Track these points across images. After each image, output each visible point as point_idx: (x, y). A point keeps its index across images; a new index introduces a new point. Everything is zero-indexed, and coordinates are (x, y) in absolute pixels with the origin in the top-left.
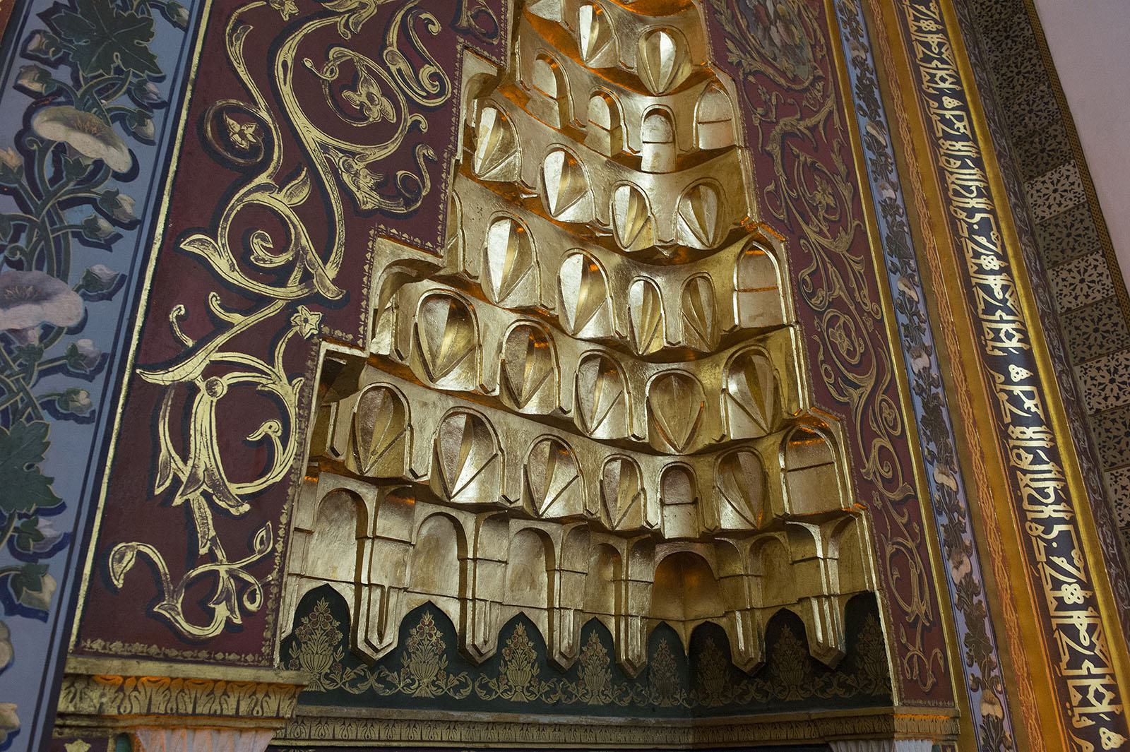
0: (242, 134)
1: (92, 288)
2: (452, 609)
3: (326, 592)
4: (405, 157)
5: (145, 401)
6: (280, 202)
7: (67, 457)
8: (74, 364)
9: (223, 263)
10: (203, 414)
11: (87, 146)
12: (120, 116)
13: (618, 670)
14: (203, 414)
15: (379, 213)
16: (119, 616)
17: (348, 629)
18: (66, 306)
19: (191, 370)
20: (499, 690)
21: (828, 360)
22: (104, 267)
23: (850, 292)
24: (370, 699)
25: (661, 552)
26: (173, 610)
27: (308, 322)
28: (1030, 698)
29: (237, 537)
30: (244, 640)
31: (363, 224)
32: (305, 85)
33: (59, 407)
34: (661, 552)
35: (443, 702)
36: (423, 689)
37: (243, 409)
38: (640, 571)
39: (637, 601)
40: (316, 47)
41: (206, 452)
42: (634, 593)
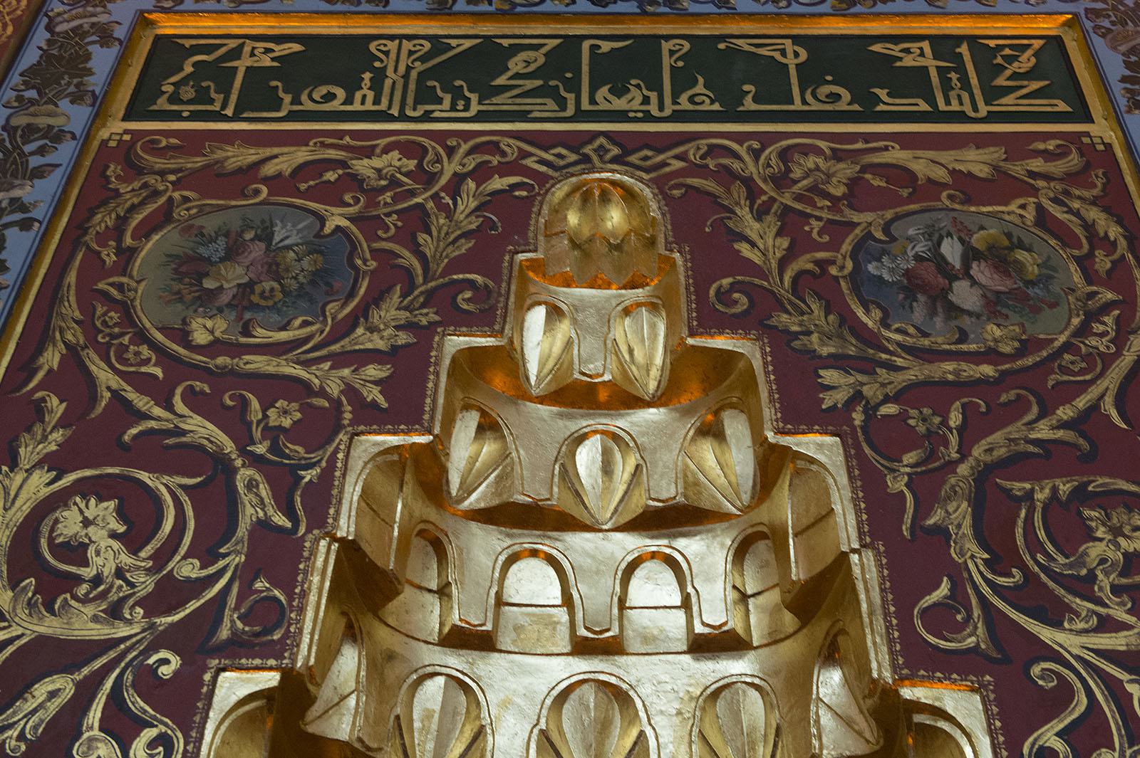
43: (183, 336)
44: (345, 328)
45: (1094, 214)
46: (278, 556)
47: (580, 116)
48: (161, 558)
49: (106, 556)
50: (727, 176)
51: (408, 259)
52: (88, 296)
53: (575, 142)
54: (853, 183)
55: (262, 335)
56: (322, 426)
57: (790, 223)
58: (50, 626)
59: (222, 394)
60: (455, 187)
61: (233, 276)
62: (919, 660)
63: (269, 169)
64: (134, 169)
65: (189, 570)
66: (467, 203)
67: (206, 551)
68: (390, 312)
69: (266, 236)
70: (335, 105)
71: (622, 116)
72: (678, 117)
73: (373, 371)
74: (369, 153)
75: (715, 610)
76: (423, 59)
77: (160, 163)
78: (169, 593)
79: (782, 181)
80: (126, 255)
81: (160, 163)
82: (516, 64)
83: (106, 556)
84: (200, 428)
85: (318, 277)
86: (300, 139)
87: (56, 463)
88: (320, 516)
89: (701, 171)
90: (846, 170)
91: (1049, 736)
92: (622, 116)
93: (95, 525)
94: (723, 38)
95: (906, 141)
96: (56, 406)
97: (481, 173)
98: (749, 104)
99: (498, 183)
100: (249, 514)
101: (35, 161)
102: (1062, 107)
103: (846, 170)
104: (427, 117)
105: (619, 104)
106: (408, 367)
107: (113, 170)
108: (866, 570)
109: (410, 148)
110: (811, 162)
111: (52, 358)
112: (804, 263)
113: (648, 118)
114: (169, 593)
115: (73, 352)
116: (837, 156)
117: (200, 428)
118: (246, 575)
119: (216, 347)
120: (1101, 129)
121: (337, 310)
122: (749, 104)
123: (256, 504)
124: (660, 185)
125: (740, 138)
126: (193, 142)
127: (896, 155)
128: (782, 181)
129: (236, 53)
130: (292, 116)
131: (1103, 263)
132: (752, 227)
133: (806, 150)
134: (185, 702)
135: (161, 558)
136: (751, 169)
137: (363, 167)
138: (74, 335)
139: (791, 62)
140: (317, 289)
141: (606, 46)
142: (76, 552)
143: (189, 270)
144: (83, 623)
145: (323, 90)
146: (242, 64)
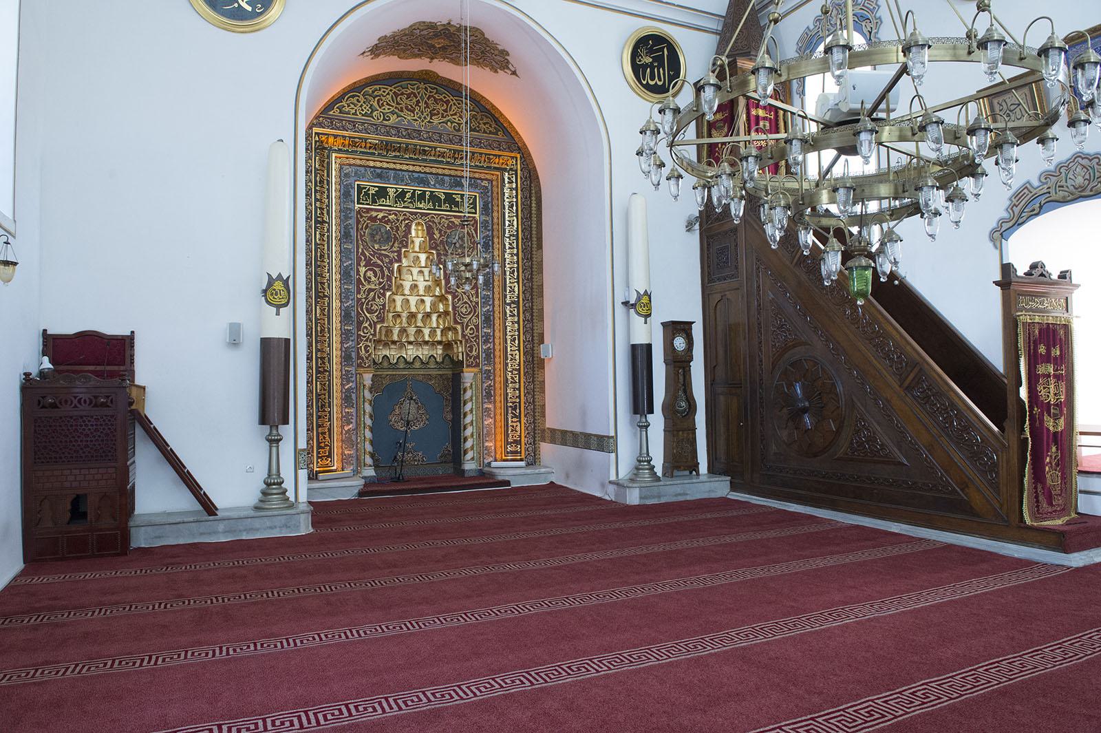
0: (361, 319)
1: (352, 341)
2: (405, 356)
3: (386, 355)
4: (380, 313)
5: (358, 348)
6: (366, 325)
7: (353, 355)
8: (352, 348)
9: (362, 334)
10: (363, 348)
11: (349, 328)
12: (351, 324)
13: (437, 362)
14: (363, 348)
15: (378, 321)
16: (359, 366)
17: (389, 360)
18: (351, 343)
19: (361, 345)
20: (414, 366)
21: (459, 315)
22: (353, 338)
23: (469, 299)
24: (393, 368)
25: (443, 344)
26: (363, 364)
27: (371, 337)
28: (498, 366)
29: (367, 358)
30: (369, 367)
31: (375, 323)
32: (367, 309)
33: (352, 351)
34: (443, 344)
35: (405, 368)
36: (401, 367)
37: (366, 347)
38: (439, 347)
39: (440, 352)
40: (367, 304)
41: (363, 352)
42: (439, 350)
43: (374, 248)
44: (392, 247)
45: (473, 232)
46: (389, 279)
47: (416, 208)
48: (379, 279)
49: (373, 279)
50: (433, 222)
51: (397, 236)
52: (362, 240)
53: (415, 214)
54: (448, 224)
55: (383, 248)
56: (391, 262)
57: (440, 231)
58: (370, 287)
59: (380, 257)
60: (401, 223)
61: (377, 237)
62: (447, 292)
63: (378, 217)
64: (362, 217)
65: (381, 280)
66: (403, 225)
67: (383, 278)
68: (396, 245)
69: (380, 231)
70: (384, 203)
71: (420, 209)
72: (428, 209)
73: (396, 254)
74: (390, 214)
75: (427, 279)
76: (395, 193)
77: (365, 215)
78: (380, 283)
79: (440, 223)
80: (364, 232)
81: (365, 215)
82: (407, 197)
83: (373, 279)
84: (379, 262)
85: (388, 238)
86: (381, 211)
87: (365, 266)
88: (393, 275)
89: (430, 221)
90: (447, 222)
91: (456, 300)
92: (420, 209)
93: (370, 274)
94: (434, 192)
95: (455, 217)
96: (363, 258)
97: (404, 220)
98: (437, 208)
99: (407, 222)
100: (386, 274)
101: (350, 215)
102: (474, 211)
103: (447, 222)
104: (396, 207)
105: (421, 206)
106: (399, 252)
107: (359, 216)
108: (443, 282)
109: (396, 215)
110: (443, 220)
111: (360, 250)
112: (441, 239)
113: (424, 209)
114: (380, 283)
115: (362, 249)
116: (446, 219)
117: (379, 262)
118: (387, 281)
119: (378, 250)
120: (477, 216)
121: (390, 244)
122: (437, 208)
123: (386, 273)
124: (425, 223)
125: (435, 214)
126: (368, 210)
127: (453, 220)
128: (440, 223)
129: (369, 190)
130: (380, 205)
131: (472, 241)
132: (436, 232)
133: (443, 218)
134: (384, 295)
135: (379, 279)
136: (436, 221)
137: (390, 217)
138: (362, 247)
139: (443, 198)
140: (388, 240)
141: (419, 192)
142: (370, 278)
143: (372, 236)
144: (373, 287)
145: (383, 199)
146: (370, 192)
